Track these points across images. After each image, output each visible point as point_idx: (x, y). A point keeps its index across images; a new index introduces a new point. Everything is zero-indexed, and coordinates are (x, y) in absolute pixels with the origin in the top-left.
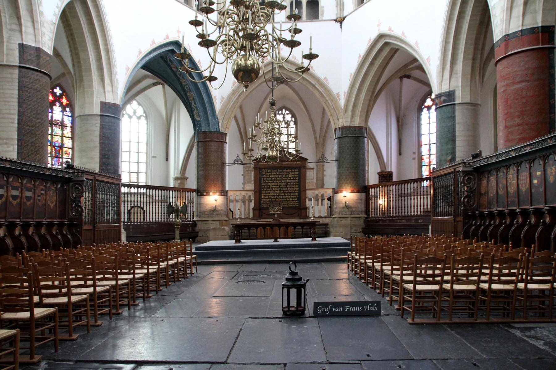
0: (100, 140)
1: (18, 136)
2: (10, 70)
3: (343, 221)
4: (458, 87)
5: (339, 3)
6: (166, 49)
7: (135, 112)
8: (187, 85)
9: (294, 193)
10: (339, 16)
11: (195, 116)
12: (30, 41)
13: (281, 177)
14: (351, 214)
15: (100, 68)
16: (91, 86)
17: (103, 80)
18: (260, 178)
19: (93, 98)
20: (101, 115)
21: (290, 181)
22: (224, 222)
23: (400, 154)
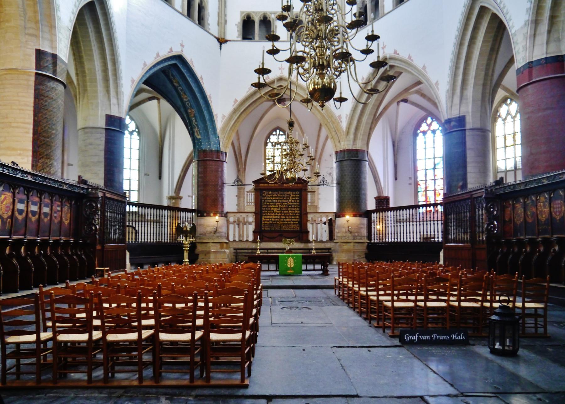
0: (105, 155)
3: (346, 247)
4: (468, 112)
6: (170, 63)
8: (189, 101)
9: (295, 216)
11: (196, 134)
14: (354, 239)
15: (106, 79)
16: (96, 98)
17: (108, 92)
18: (261, 200)
20: (106, 129)
21: (291, 204)
22: (225, 245)
23: (396, 179)
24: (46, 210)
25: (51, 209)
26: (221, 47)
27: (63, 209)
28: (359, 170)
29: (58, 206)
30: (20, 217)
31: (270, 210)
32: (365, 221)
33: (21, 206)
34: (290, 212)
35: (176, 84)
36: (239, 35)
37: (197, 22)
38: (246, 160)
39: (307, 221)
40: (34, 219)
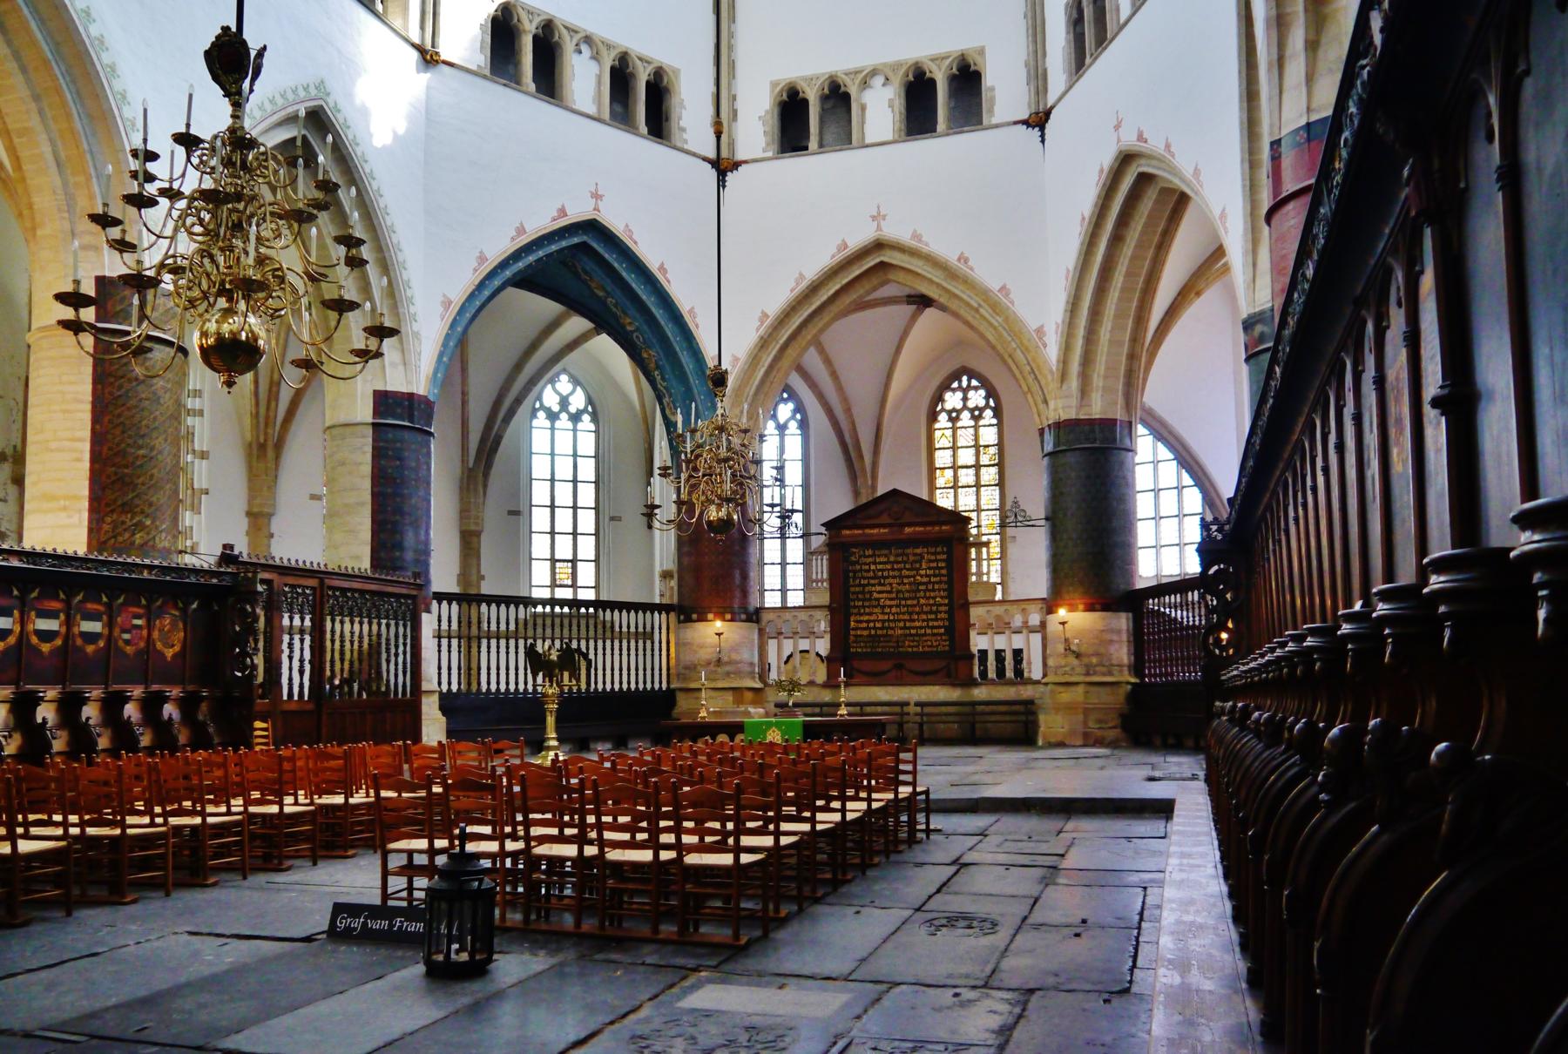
3: (1066, 696)
7: (564, 402)
8: (637, 330)
9: (936, 613)
14: (1088, 674)
18: (846, 572)
32: (1123, 621)
34: (922, 601)
37: (644, 129)
39: (968, 626)
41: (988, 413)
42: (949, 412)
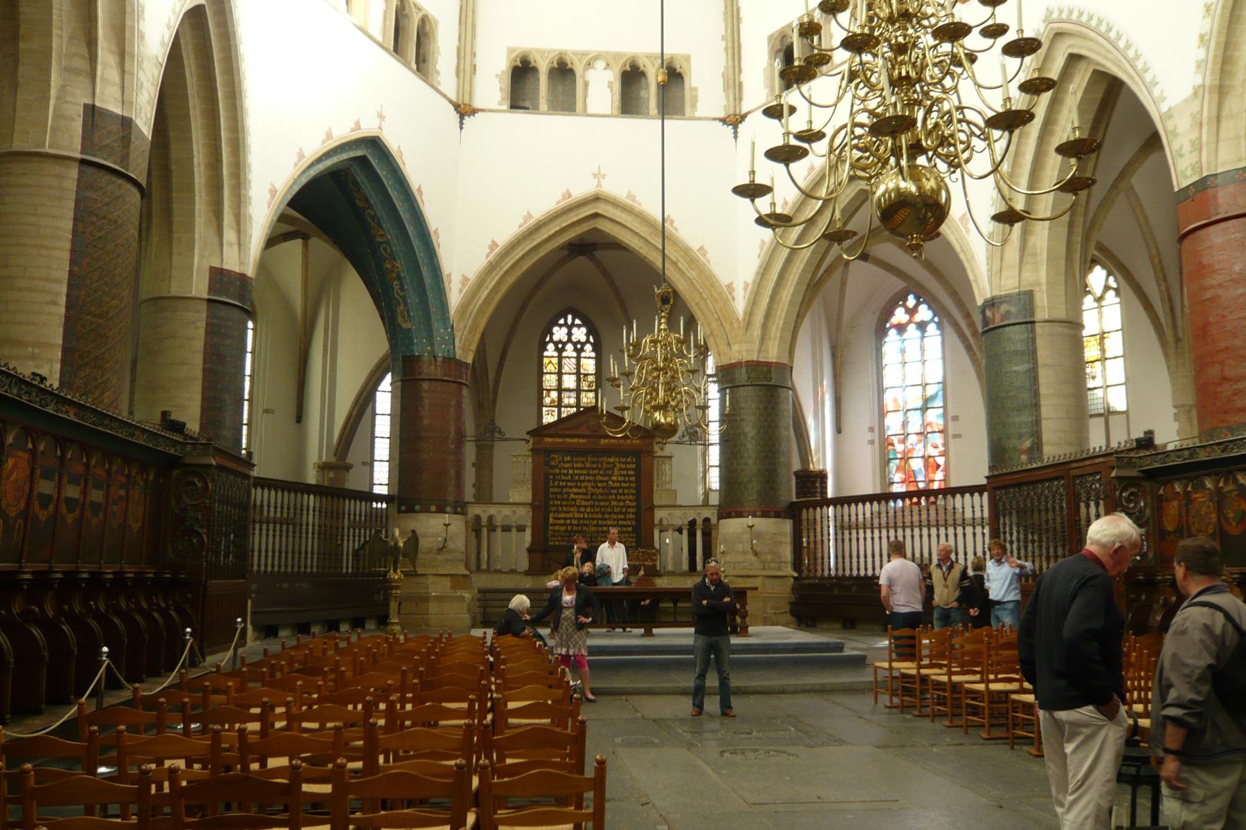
0: (205, 362)
1: (64, 340)
2: (58, 168)
5: (731, 82)
6: (352, 154)
9: (625, 514)
10: (731, 112)
11: (400, 319)
12: (109, 101)
13: (595, 475)
16: (190, 227)
17: (218, 214)
18: (547, 475)
19: (193, 256)
20: (209, 301)
21: (617, 485)
24: (97, 496)
25: (107, 496)
26: (461, 124)
27: (131, 493)
28: (773, 408)
29: (121, 487)
30: (42, 515)
31: (567, 500)
32: (787, 526)
33: (46, 487)
34: (613, 503)
35: (360, 203)
36: (503, 99)
37: (414, 66)
38: (497, 381)
40: (70, 518)
41: (588, 347)
42: (556, 344)
